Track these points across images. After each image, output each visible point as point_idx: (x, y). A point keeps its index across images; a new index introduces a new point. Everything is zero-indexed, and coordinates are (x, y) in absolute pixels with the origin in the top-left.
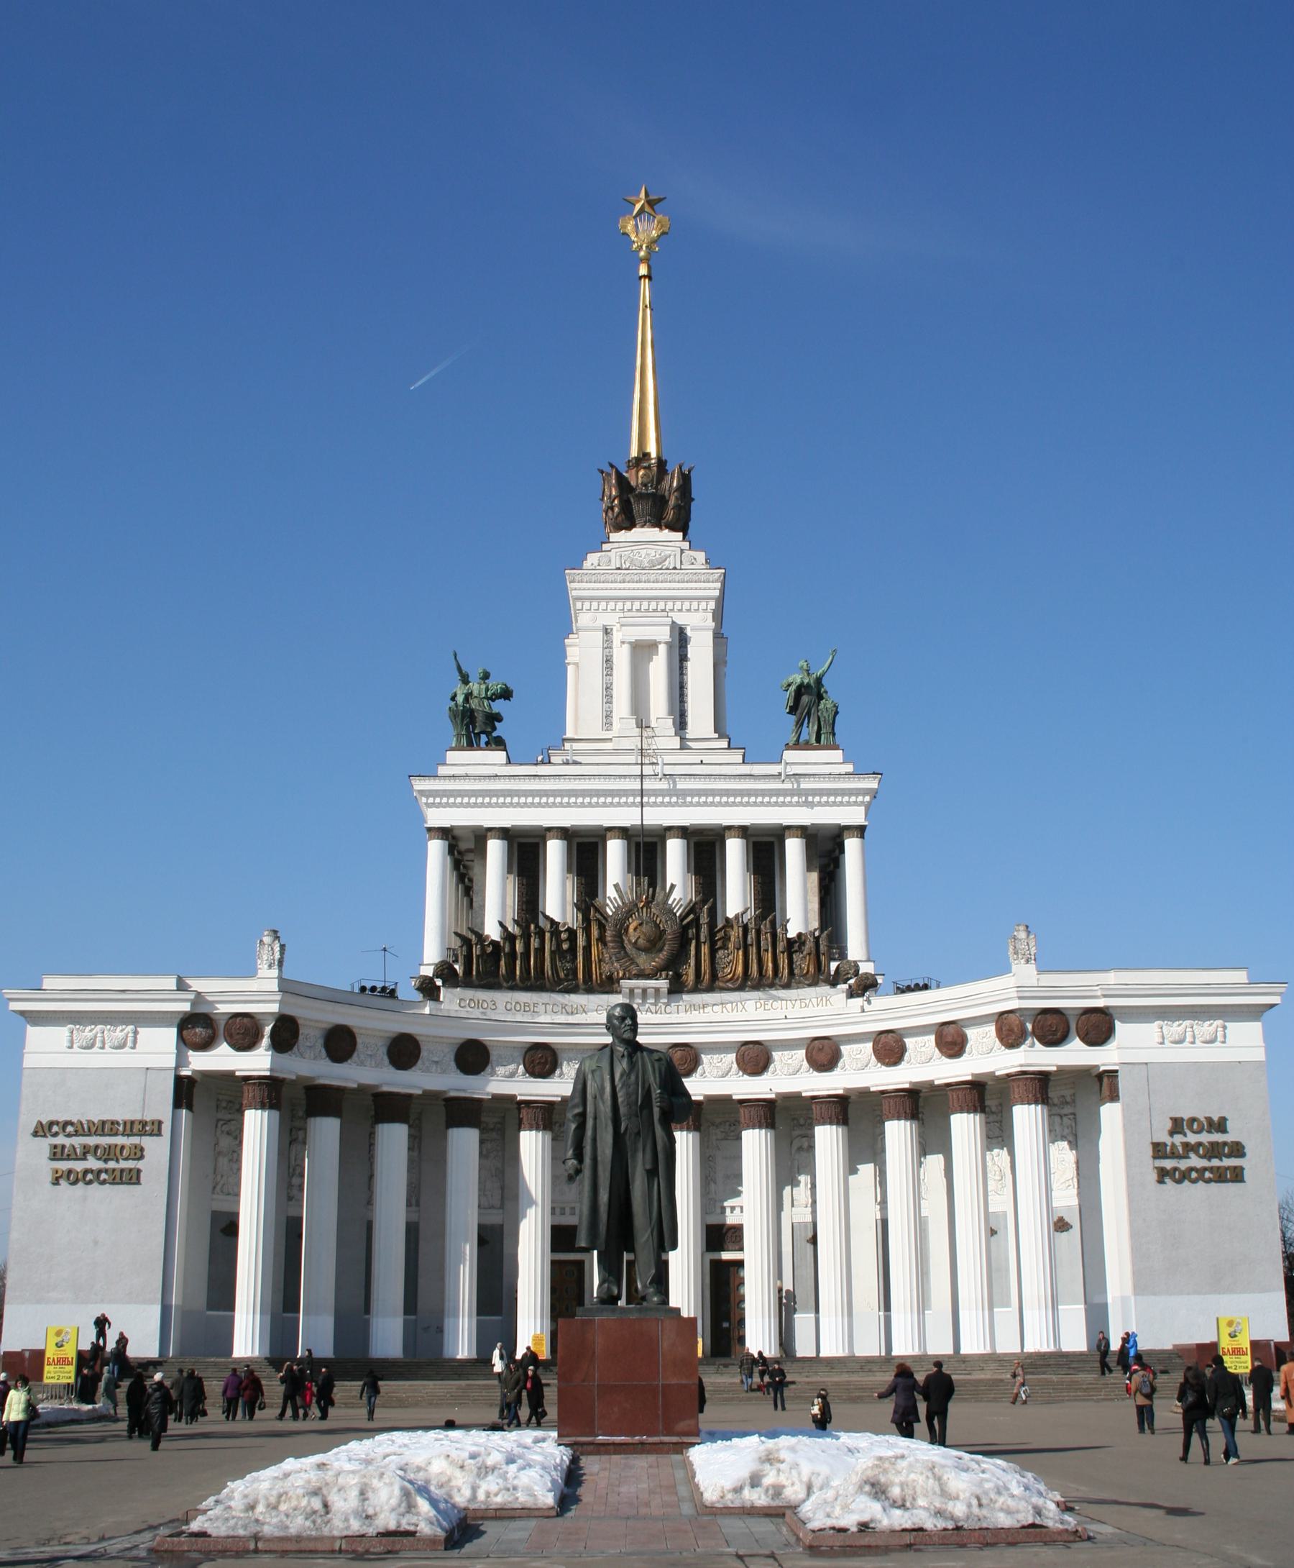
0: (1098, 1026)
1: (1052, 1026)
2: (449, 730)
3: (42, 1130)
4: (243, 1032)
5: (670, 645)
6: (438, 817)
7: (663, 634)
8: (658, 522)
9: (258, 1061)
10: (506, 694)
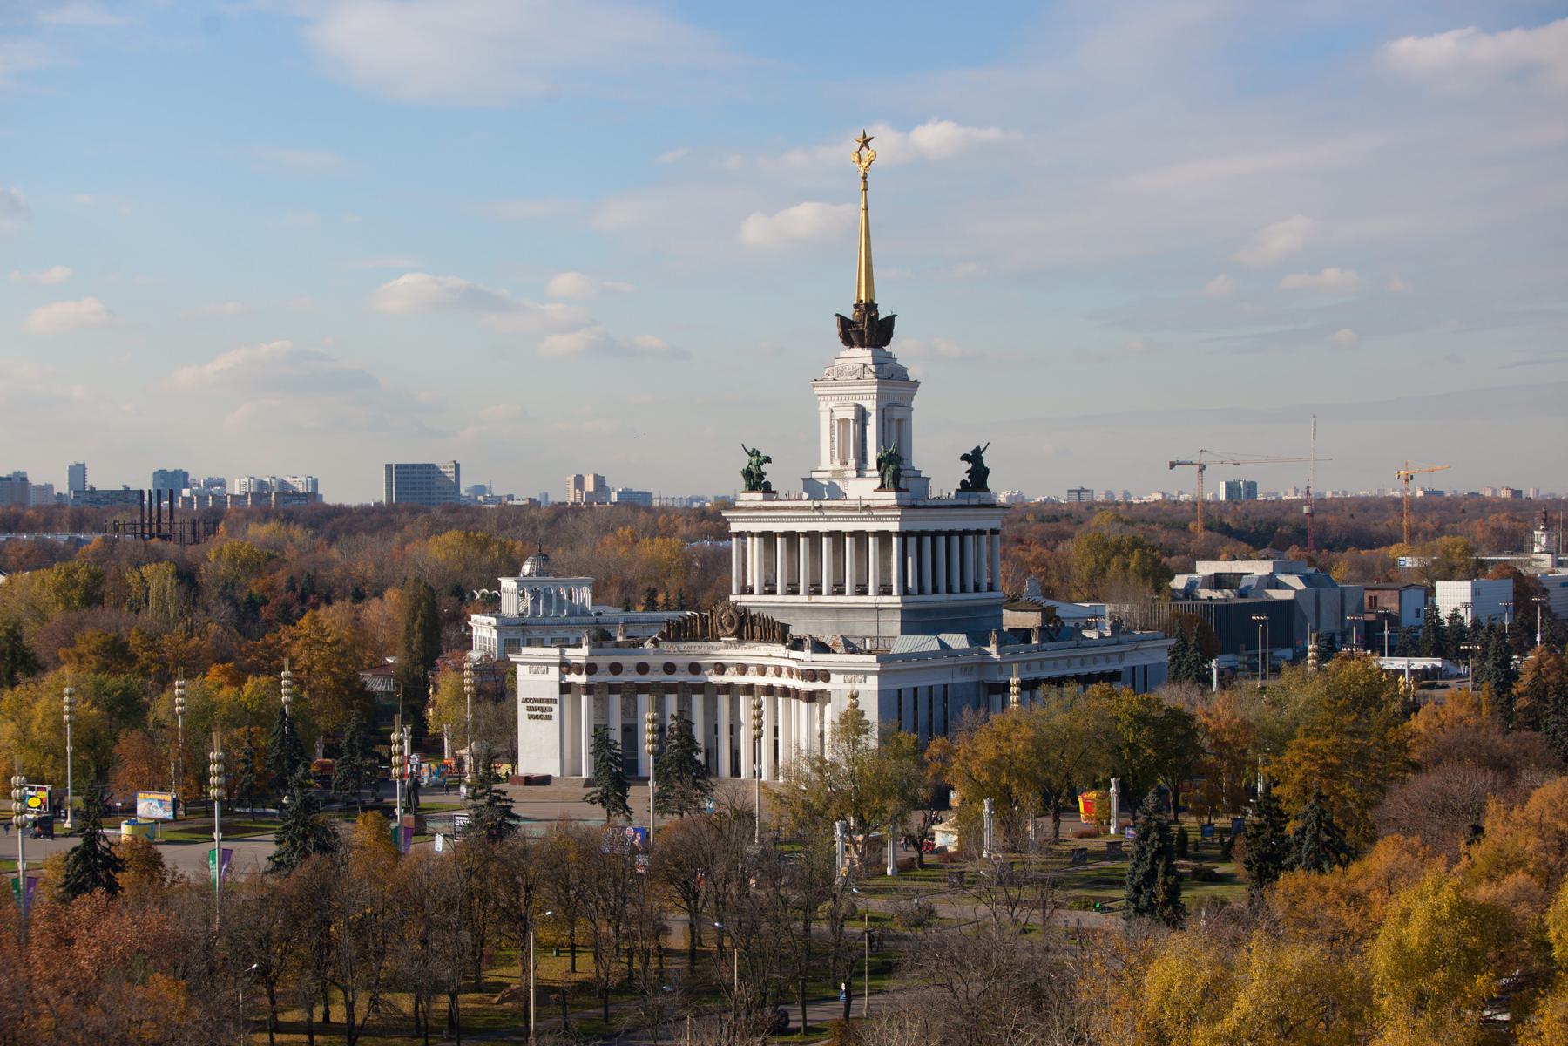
0: (826, 676)
1: (811, 675)
2: (742, 482)
3: (525, 701)
4: (578, 669)
5: (856, 421)
6: (734, 528)
7: (851, 415)
8: (863, 346)
9: (581, 679)
10: (768, 460)
